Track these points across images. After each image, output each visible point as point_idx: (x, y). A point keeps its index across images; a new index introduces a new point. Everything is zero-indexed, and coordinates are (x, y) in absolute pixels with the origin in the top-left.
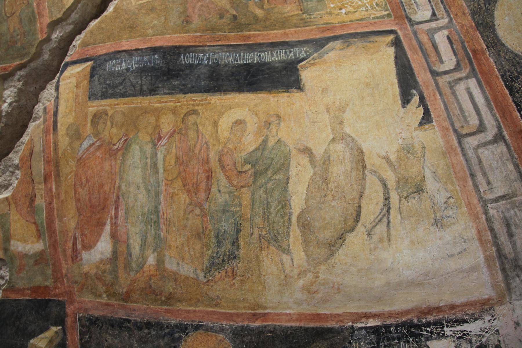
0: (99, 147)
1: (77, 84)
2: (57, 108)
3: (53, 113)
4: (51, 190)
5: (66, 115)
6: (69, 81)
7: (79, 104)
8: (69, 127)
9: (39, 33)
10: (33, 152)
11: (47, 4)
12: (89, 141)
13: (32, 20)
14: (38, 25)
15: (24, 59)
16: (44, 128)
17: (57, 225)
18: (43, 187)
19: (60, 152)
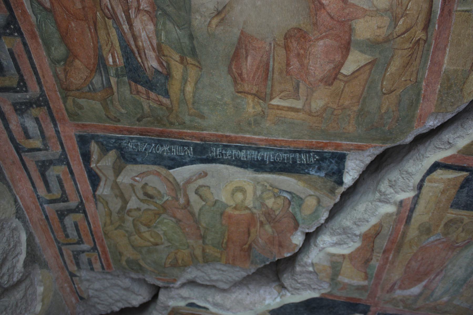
0: (443, 242)
1: (443, 190)
2: (415, 205)
3: (409, 208)
4: (387, 258)
5: (423, 215)
6: (436, 185)
7: (439, 208)
8: (422, 224)
9: (416, 121)
10: (380, 233)
11: (439, 86)
12: (436, 237)
13: (414, 105)
14: (419, 111)
15: (386, 143)
16: (396, 218)
17: (384, 276)
18: (381, 256)
19: (407, 239)
